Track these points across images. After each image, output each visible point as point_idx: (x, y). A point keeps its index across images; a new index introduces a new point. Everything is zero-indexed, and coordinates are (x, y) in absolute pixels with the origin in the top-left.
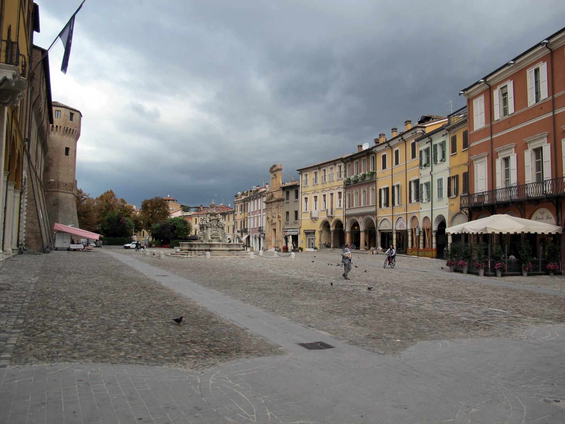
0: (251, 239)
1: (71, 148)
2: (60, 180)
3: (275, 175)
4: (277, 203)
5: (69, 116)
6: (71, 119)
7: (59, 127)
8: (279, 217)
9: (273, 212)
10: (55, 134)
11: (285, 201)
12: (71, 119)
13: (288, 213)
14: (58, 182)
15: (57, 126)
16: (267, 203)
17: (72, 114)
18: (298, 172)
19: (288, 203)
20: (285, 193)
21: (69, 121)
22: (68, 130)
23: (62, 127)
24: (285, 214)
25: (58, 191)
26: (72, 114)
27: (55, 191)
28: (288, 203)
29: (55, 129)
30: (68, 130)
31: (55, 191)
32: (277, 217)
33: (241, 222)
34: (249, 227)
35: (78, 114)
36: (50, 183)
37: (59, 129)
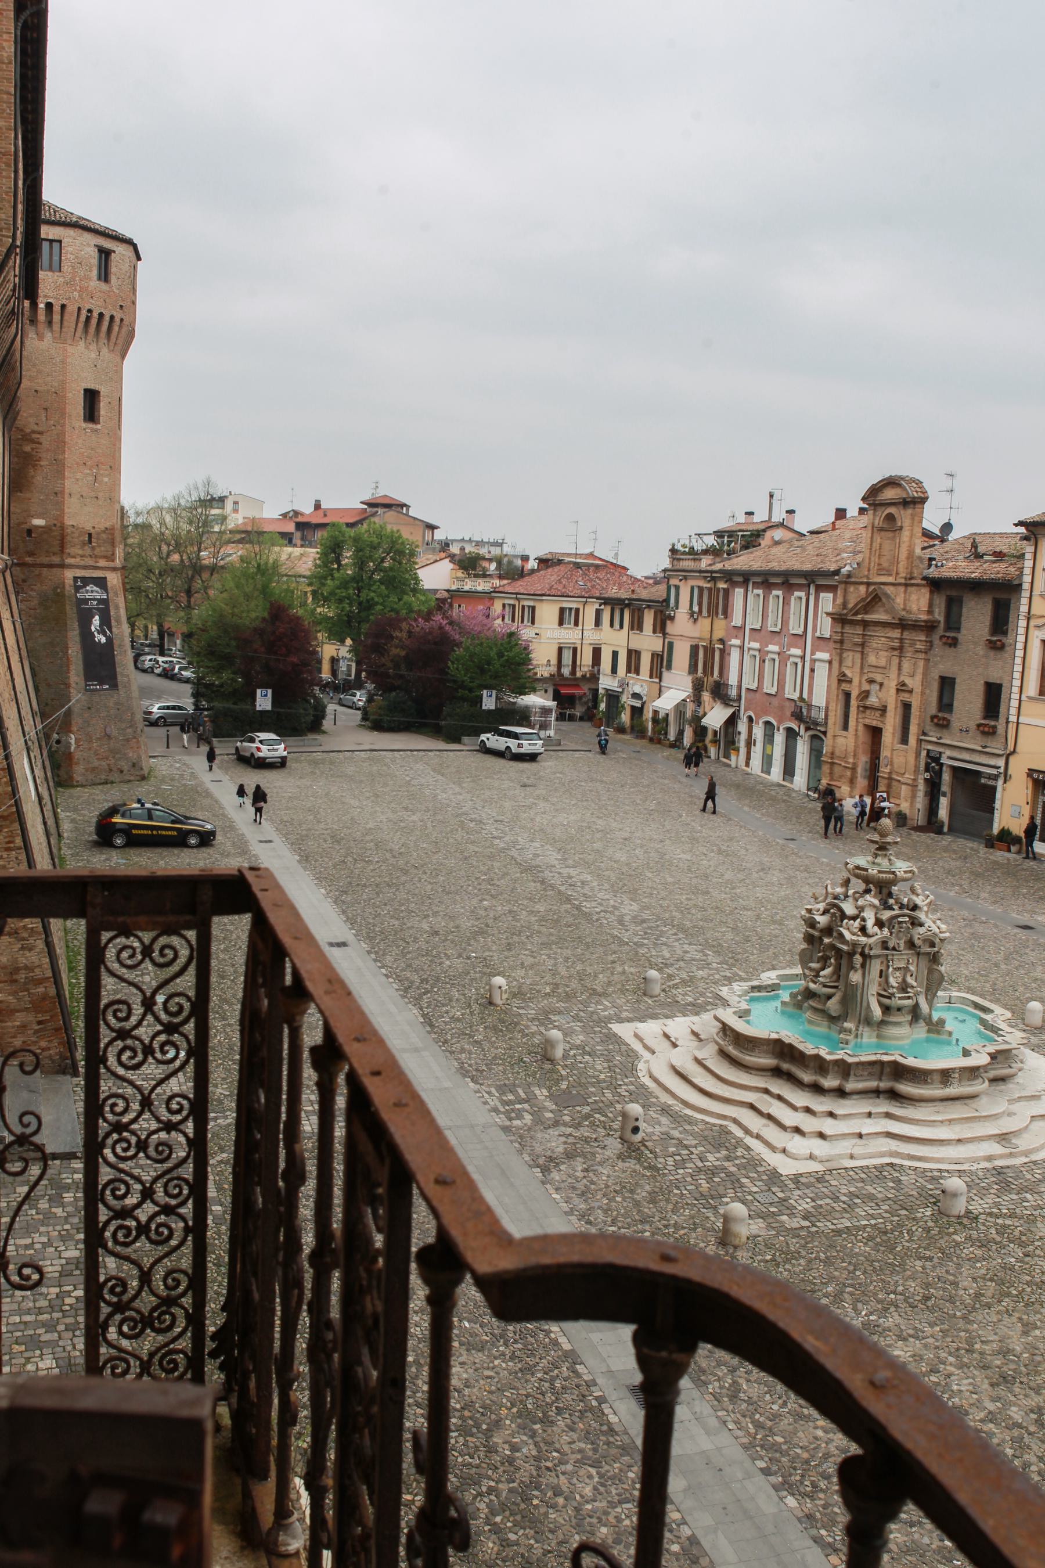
0: (742, 727)
1: (104, 391)
2: (68, 522)
3: (890, 518)
4: (896, 634)
5: (95, 261)
6: (104, 275)
7: (57, 309)
8: (902, 688)
9: (872, 659)
10: (41, 337)
11: (940, 630)
12: (104, 275)
13: (947, 684)
14: (63, 528)
15: (49, 306)
16: (840, 619)
17: (105, 254)
18: (1022, 530)
19: (954, 643)
20: (940, 603)
21: (94, 283)
22: (94, 322)
23: (72, 308)
24: (935, 686)
25: (62, 566)
26: (105, 254)
27: (51, 566)
28: (954, 643)
29: (42, 316)
30: (94, 322)
31: (51, 566)
32: (892, 685)
33: (694, 649)
34: (733, 679)
35: (128, 251)
36: (29, 532)
37: (56, 317)
